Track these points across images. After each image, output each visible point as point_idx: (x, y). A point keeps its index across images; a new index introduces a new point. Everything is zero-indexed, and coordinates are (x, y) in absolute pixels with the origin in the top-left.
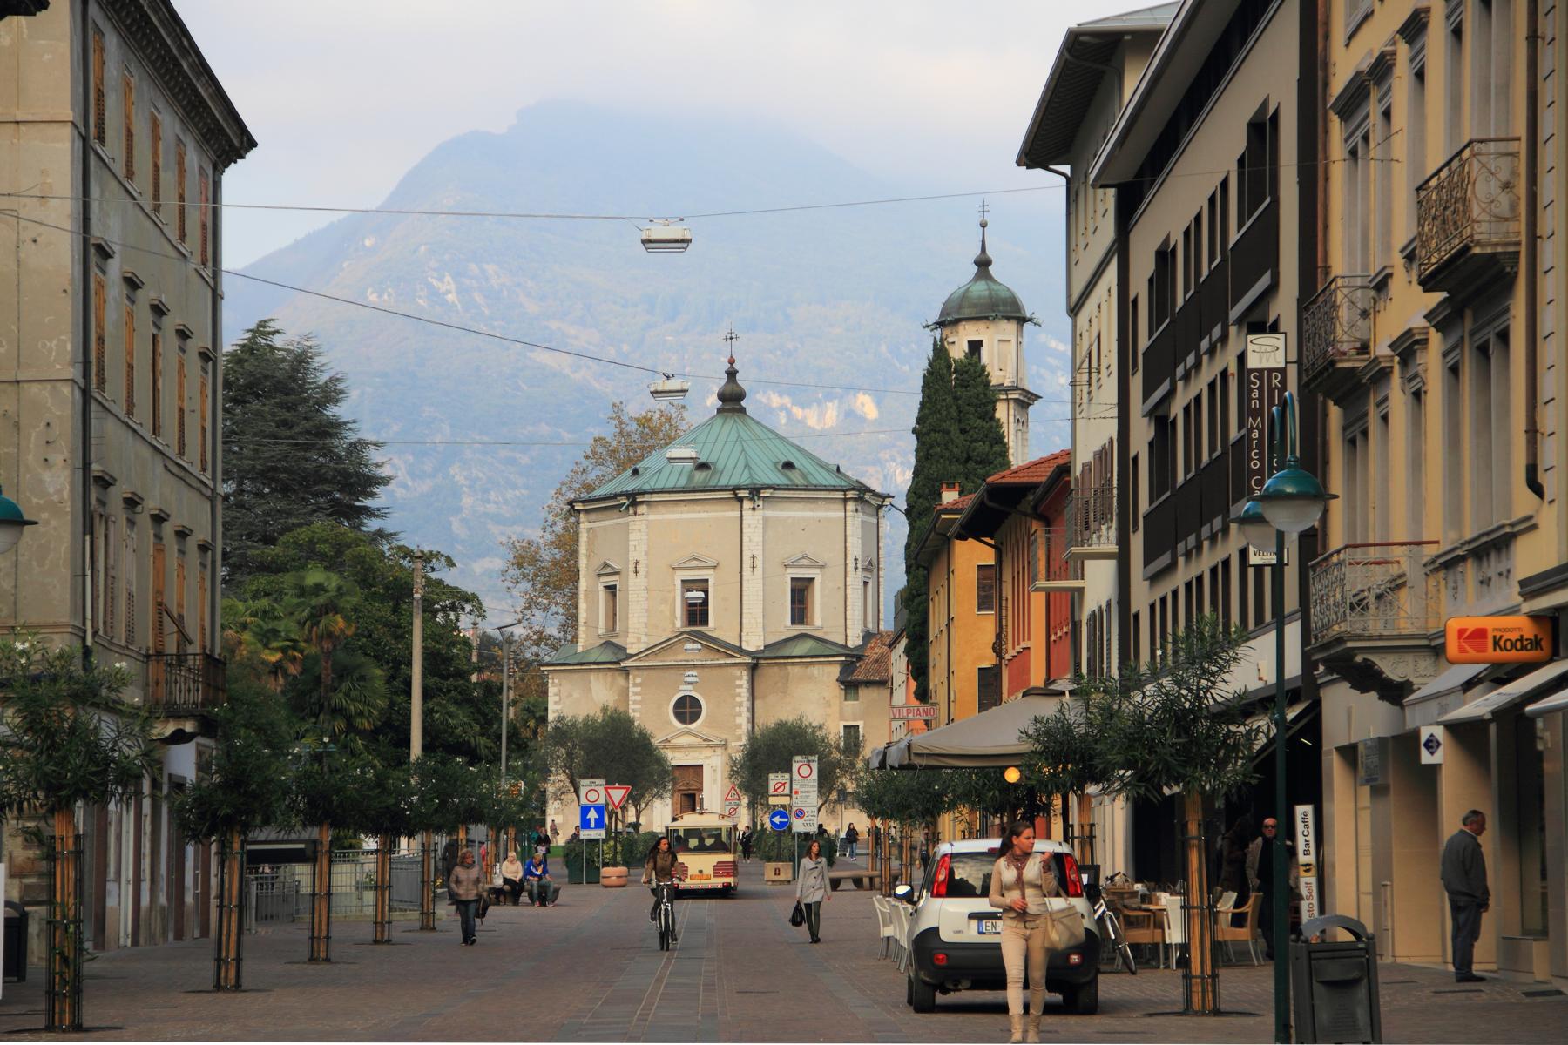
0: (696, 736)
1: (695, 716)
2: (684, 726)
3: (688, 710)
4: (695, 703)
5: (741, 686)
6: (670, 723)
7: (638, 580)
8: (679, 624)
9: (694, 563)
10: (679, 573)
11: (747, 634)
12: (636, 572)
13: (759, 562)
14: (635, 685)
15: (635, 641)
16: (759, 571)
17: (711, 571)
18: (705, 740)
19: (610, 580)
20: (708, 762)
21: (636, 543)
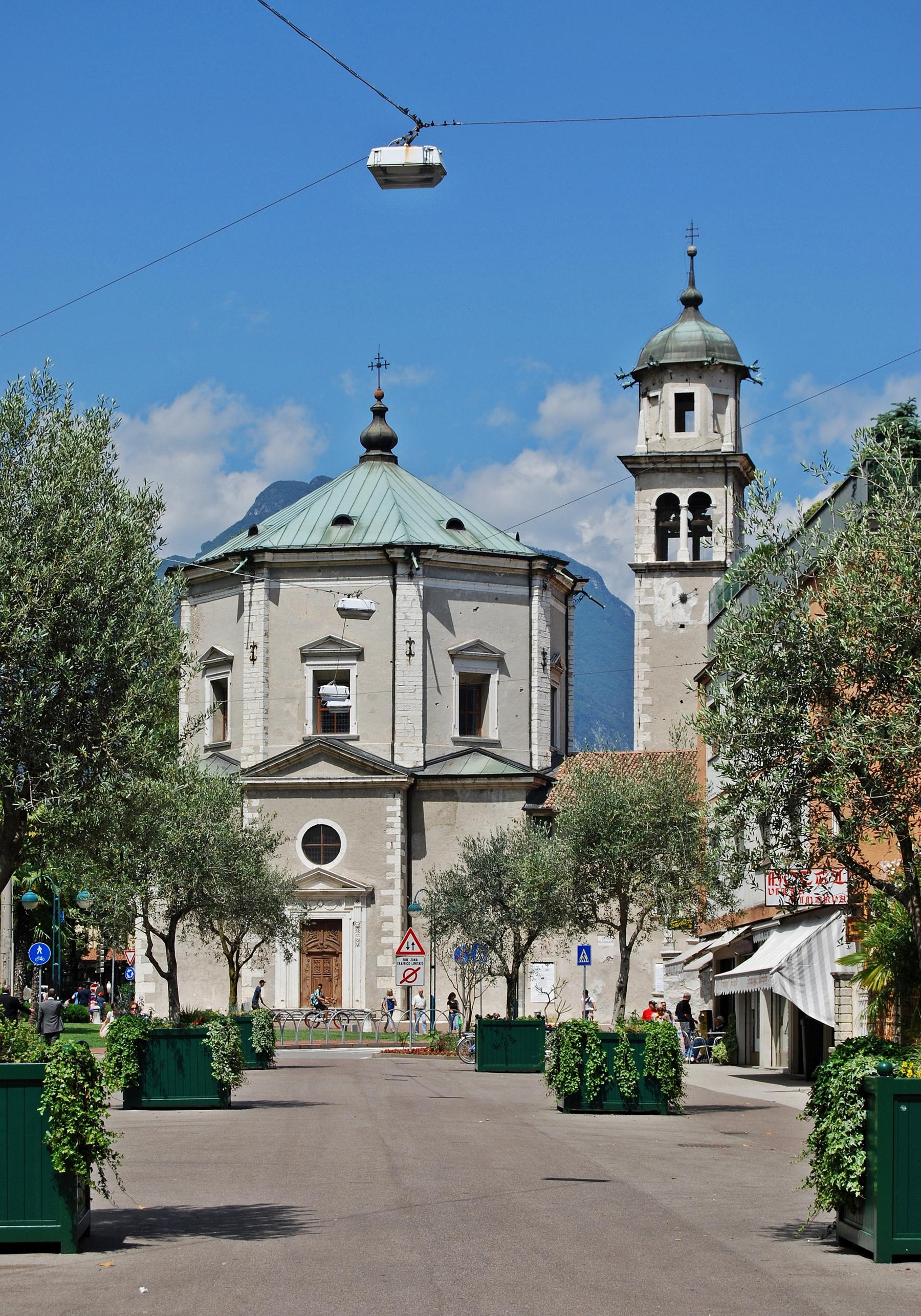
1: (331, 853)
2: (316, 866)
5: (393, 814)
6: (298, 862)
7: (255, 669)
11: (402, 745)
12: (253, 660)
14: (251, 810)
15: (252, 751)
20: (348, 915)
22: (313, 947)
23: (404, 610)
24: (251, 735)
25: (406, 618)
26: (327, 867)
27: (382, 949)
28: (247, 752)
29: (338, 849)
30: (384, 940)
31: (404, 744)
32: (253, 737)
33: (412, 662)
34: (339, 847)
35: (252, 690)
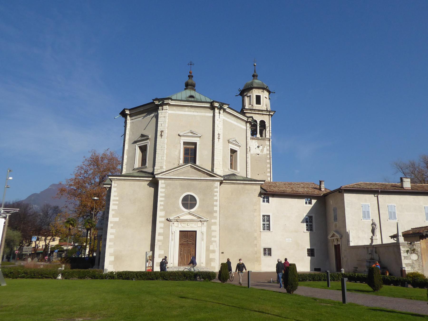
1: (193, 205)
3: (189, 202)
4: (193, 199)
7: (162, 140)
8: (181, 162)
10: (182, 138)
11: (216, 168)
13: (221, 137)
16: (221, 140)
17: (198, 139)
18: (199, 218)
21: (162, 123)
22: (184, 242)
25: (218, 127)
26: (192, 210)
28: (157, 168)
29: (196, 204)
30: (213, 239)
31: (217, 169)
32: (160, 163)
34: (196, 203)
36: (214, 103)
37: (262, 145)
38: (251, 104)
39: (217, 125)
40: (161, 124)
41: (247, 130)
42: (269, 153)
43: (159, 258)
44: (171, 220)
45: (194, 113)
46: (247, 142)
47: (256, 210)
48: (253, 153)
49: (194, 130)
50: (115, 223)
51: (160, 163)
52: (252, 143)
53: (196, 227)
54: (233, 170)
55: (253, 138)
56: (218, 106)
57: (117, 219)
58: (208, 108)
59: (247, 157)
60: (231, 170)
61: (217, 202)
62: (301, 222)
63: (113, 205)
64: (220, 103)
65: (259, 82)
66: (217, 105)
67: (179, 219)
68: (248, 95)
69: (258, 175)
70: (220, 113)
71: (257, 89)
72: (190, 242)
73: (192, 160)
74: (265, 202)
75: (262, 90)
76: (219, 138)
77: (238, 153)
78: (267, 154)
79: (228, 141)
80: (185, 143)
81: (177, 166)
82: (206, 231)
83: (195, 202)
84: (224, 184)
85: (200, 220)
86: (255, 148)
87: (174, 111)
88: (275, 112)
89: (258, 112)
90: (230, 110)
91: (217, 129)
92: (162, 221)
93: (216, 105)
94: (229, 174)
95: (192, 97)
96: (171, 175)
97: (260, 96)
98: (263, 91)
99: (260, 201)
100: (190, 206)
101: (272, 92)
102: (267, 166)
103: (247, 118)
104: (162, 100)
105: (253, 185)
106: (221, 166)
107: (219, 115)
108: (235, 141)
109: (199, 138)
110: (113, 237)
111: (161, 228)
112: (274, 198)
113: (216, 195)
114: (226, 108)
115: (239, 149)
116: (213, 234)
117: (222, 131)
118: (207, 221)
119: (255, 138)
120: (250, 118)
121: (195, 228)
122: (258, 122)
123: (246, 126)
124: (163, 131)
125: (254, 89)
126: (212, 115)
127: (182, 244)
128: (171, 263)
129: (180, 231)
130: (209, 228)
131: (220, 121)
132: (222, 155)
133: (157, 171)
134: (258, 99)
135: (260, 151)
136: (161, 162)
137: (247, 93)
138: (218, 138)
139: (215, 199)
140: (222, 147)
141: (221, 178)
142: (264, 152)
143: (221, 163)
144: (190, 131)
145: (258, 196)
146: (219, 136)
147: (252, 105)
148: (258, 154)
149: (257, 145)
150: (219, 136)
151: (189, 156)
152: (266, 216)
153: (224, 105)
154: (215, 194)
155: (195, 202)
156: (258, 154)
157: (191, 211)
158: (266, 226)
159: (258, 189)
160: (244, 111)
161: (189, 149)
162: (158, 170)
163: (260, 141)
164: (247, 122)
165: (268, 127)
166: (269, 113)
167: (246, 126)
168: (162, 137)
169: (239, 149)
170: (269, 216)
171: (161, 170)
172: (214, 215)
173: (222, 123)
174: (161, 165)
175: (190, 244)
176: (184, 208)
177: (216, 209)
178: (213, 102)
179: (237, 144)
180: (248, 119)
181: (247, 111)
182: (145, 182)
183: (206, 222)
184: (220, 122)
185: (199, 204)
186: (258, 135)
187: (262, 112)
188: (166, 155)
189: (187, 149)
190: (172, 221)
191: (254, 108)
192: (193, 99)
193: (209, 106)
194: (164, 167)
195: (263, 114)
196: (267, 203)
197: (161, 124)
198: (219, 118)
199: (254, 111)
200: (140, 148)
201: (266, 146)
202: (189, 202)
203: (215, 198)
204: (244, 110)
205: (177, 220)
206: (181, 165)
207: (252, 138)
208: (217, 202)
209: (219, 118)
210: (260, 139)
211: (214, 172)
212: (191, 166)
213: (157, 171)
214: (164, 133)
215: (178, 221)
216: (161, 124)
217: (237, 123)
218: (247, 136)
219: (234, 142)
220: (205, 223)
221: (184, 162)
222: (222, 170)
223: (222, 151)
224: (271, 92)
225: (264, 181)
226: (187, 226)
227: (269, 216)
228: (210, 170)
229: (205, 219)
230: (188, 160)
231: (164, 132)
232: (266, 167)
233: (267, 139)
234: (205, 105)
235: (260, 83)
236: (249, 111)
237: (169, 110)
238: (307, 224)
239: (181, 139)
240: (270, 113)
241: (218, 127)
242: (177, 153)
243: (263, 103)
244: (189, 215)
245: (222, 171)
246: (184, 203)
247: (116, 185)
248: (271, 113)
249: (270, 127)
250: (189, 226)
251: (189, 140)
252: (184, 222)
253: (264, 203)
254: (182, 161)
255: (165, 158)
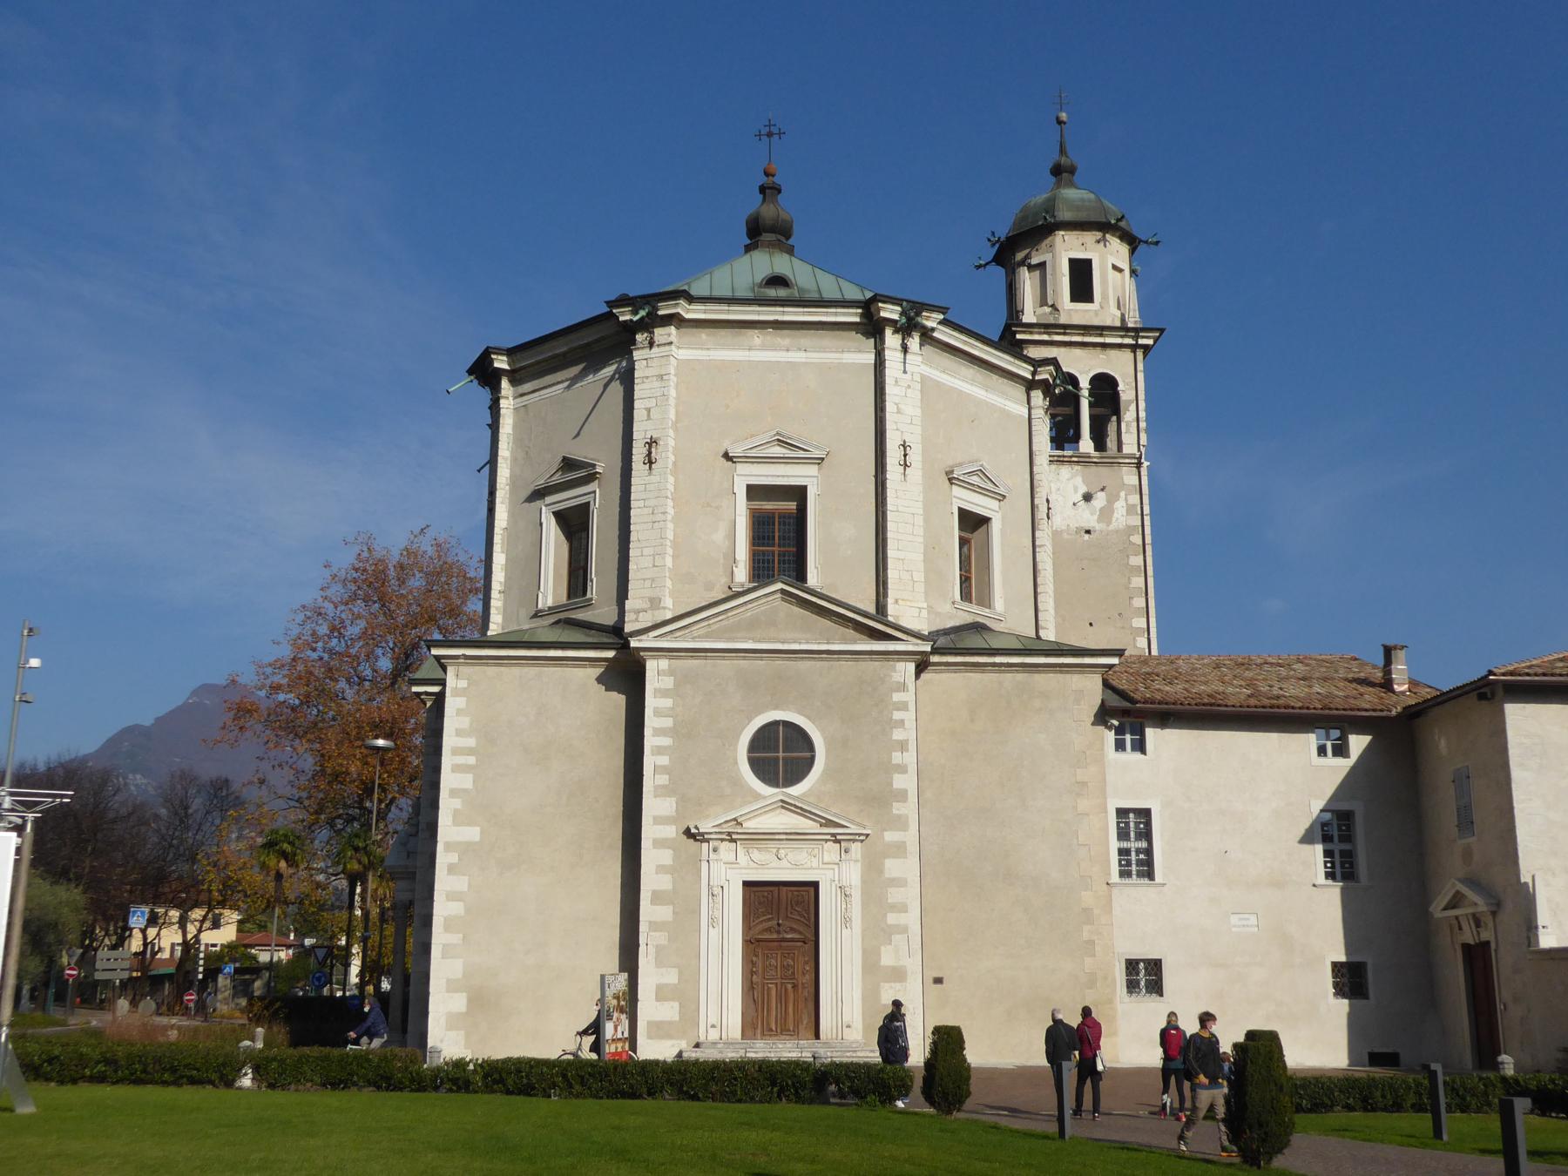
0: (803, 812)
3: (781, 754)
4: (798, 739)
8: (742, 575)
9: (778, 451)
11: (896, 601)
13: (915, 457)
15: (646, 605)
16: (915, 472)
18: (830, 823)
19: (568, 499)
23: (897, 400)
24: (644, 580)
25: (899, 412)
27: (888, 933)
29: (810, 762)
30: (892, 919)
31: (900, 602)
32: (648, 584)
33: (908, 478)
35: (646, 511)
36: (880, 305)
37: (1102, 490)
38: (1050, 303)
39: (896, 404)
40: (646, 409)
41: (1034, 422)
42: (1140, 524)
43: (657, 999)
44: (702, 834)
45: (790, 354)
46: (1036, 477)
47: (1084, 784)
48: (1063, 528)
49: (793, 431)
50: (465, 849)
51: (648, 584)
52: (1058, 480)
53: (815, 864)
54: (974, 608)
55: (1064, 456)
56: (896, 317)
57: (472, 833)
58: (853, 327)
59: (1037, 543)
60: (966, 606)
61: (907, 750)
62: (1298, 839)
63: (453, 771)
64: (905, 303)
65: (1083, 200)
66: (892, 311)
67: (739, 831)
68: (1034, 261)
69: (1091, 624)
70: (905, 349)
71: (1074, 233)
72: (793, 930)
73: (787, 566)
74: (1124, 749)
75: (1099, 235)
76: (906, 465)
77: (996, 527)
78: (1128, 527)
79: (947, 473)
80: (754, 492)
81: (724, 596)
82: (859, 884)
83: (808, 754)
84: (935, 672)
85: (833, 835)
86: (1074, 504)
87: (702, 349)
88: (1162, 331)
89: (1083, 335)
90: (954, 333)
91: (896, 423)
92: (666, 839)
93: (890, 312)
94: (958, 624)
95: (777, 281)
96: (699, 637)
97: (1088, 263)
98: (1104, 236)
99: (1103, 744)
100: (785, 772)
101: (1146, 242)
102: (1131, 586)
103: (1032, 369)
104: (648, 303)
105: (1068, 672)
106: (921, 588)
107: (905, 359)
108: (981, 472)
109: (817, 466)
110: (456, 908)
111: (661, 869)
112: (1168, 732)
113: (902, 721)
114: (934, 325)
115: (997, 509)
116: (895, 895)
117: (918, 430)
118: (862, 838)
119: (1071, 457)
120: (1048, 368)
121: (811, 868)
122: (1084, 384)
123: (1029, 403)
124: (655, 442)
125: (1062, 233)
126: (870, 358)
127: (759, 941)
128: (713, 1026)
129: (746, 884)
130: (873, 868)
131: (909, 387)
132: (921, 540)
133: (637, 620)
134: (1081, 274)
135: (1096, 517)
136: (653, 580)
137: (1029, 253)
138: (902, 463)
139: (895, 737)
140: (920, 505)
141: (919, 642)
142: (1114, 519)
143: (919, 576)
144: (775, 435)
145: (1093, 724)
146: (905, 455)
147: (1053, 306)
148: (1088, 532)
149: (1083, 489)
150: (905, 455)
151: (776, 549)
152: (1131, 815)
153: (924, 314)
154: (897, 715)
155: (808, 754)
156: (1088, 532)
157: (789, 796)
158: (1133, 857)
159: (1090, 690)
160: (1019, 336)
161: (774, 518)
162: (641, 614)
163: (1093, 469)
164: (1030, 385)
165: (1130, 402)
166: (1132, 337)
167: (1029, 403)
168: (653, 466)
169: (997, 509)
170: (1145, 814)
171: (653, 616)
172: (895, 811)
173: (919, 395)
174: (648, 593)
175: (792, 940)
176: (759, 778)
177: (900, 782)
178: (875, 299)
179: (990, 486)
180: (1034, 374)
181: (1031, 333)
182: (584, 666)
183: (859, 844)
184: (909, 391)
185: (826, 764)
186: (1086, 445)
187: (1101, 335)
188: (675, 545)
189: (764, 517)
190: (708, 841)
191: (1063, 320)
192: (782, 293)
193: (857, 319)
194: (668, 602)
195: (1104, 346)
196: (1138, 756)
197: (648, 410)
198: (905, 372)
199: (1064, 334)
200: (560, 516)
201: (1123, 494)
202: (781, 754)
203: (898, 735)
204: (1015, 333)
205: (729, 834)
206: (741, 590)
207: (1059, 456)
208: (907, 750)
209: (905, 372)
210: (1095, 460)
211: (890, 618)
212: (783, 591)
213: (637, 620)
214: (660, 448)
215: (735, 841)
216: (646, 409)
217: (987, 391)
218: (1034, 448)
219: (975, 480)
220: (856, 848)
221: (754, 577)
222: (925, 605)
223: (920, 521)
224: (1140, 241)
225: (1119, 653)
226: (776, 863)
227: (1145, 814)
228: (872, 609)
229: (854, 829)
230: (771, 565)
231: (661, 443)
232: (1128, 588)
233: (1127, 461)
234: (836, 314)
235: (1090, 201)
236: (1040, 333)
237: (678, 348)
238: (1330, 846)
239: (738, 472)
240: (1136, 338)
241: (899, 412)
242: (720, 536)
243: (1105, 296)
244: (783, 811)
245: (924, 613)
246: (758, 759)
247: (463, 684)
248: (1143, 337)
249: (1142, 405)
250: (784, 863)
251: (770, 479)
252: (762, 845)
253: (1121, 756)
254: (744, 570)
255: (669, 562)
